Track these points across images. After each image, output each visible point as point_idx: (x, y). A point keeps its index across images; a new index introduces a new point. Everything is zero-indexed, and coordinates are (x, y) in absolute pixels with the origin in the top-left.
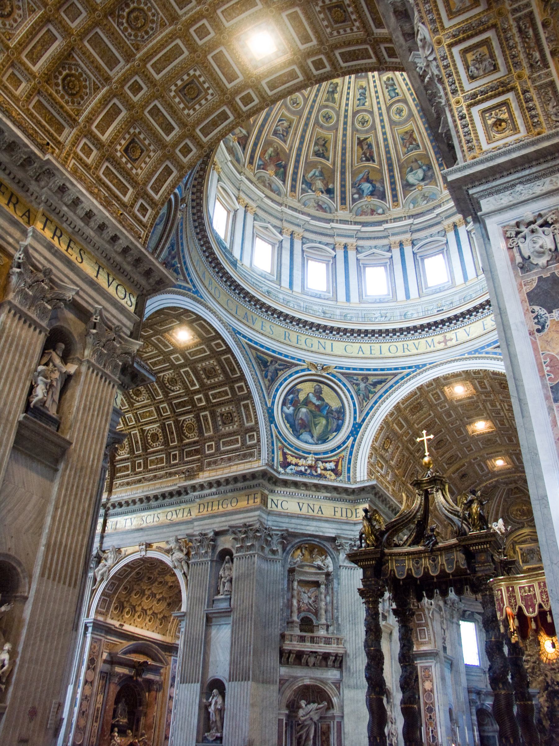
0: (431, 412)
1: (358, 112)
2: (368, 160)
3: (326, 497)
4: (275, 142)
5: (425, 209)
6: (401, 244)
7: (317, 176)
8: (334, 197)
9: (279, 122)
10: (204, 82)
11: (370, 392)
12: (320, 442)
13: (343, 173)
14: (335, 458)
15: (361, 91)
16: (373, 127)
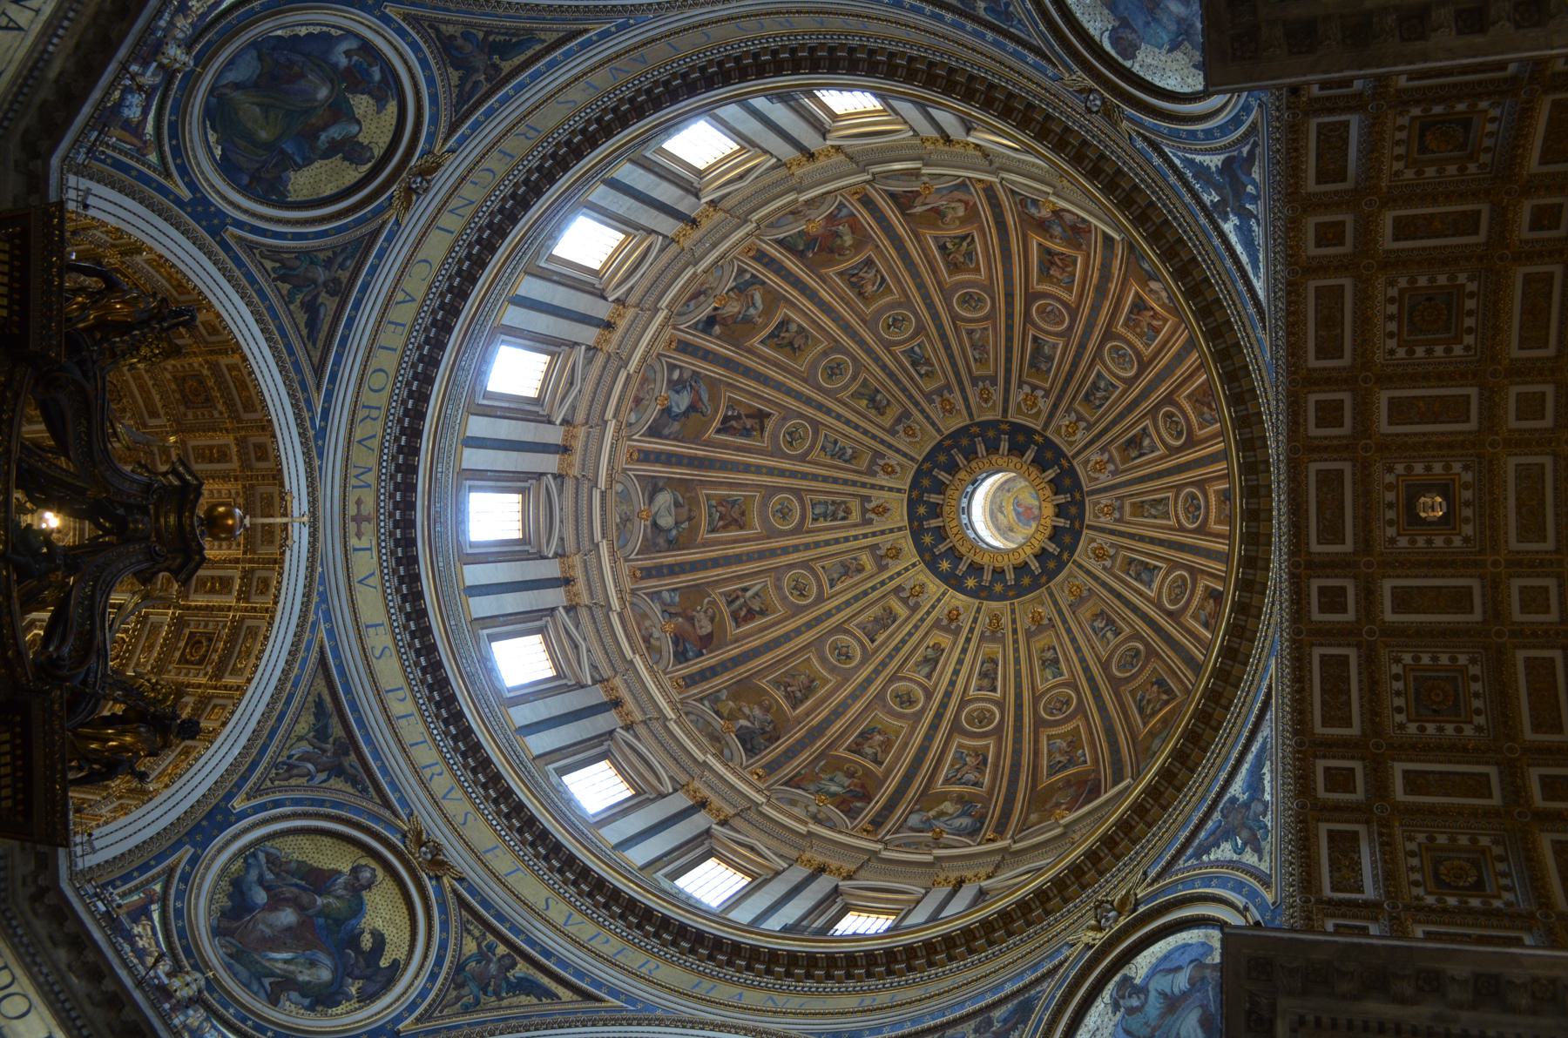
0: (163, 421)
1: (816, 433)
2: (726, 419)
3: (48, 62)
4: (855, 256)
5: (609, 516)
6: (565, 450)
7: (748, 308)
8: (696, 329)
9: (883, 277)
10: (1430, 352)
11: (297, 288)
12: (213, 100)
13: (727, 363)
14: (149, 127)
15: (850, 451)
16: (777, 453)
